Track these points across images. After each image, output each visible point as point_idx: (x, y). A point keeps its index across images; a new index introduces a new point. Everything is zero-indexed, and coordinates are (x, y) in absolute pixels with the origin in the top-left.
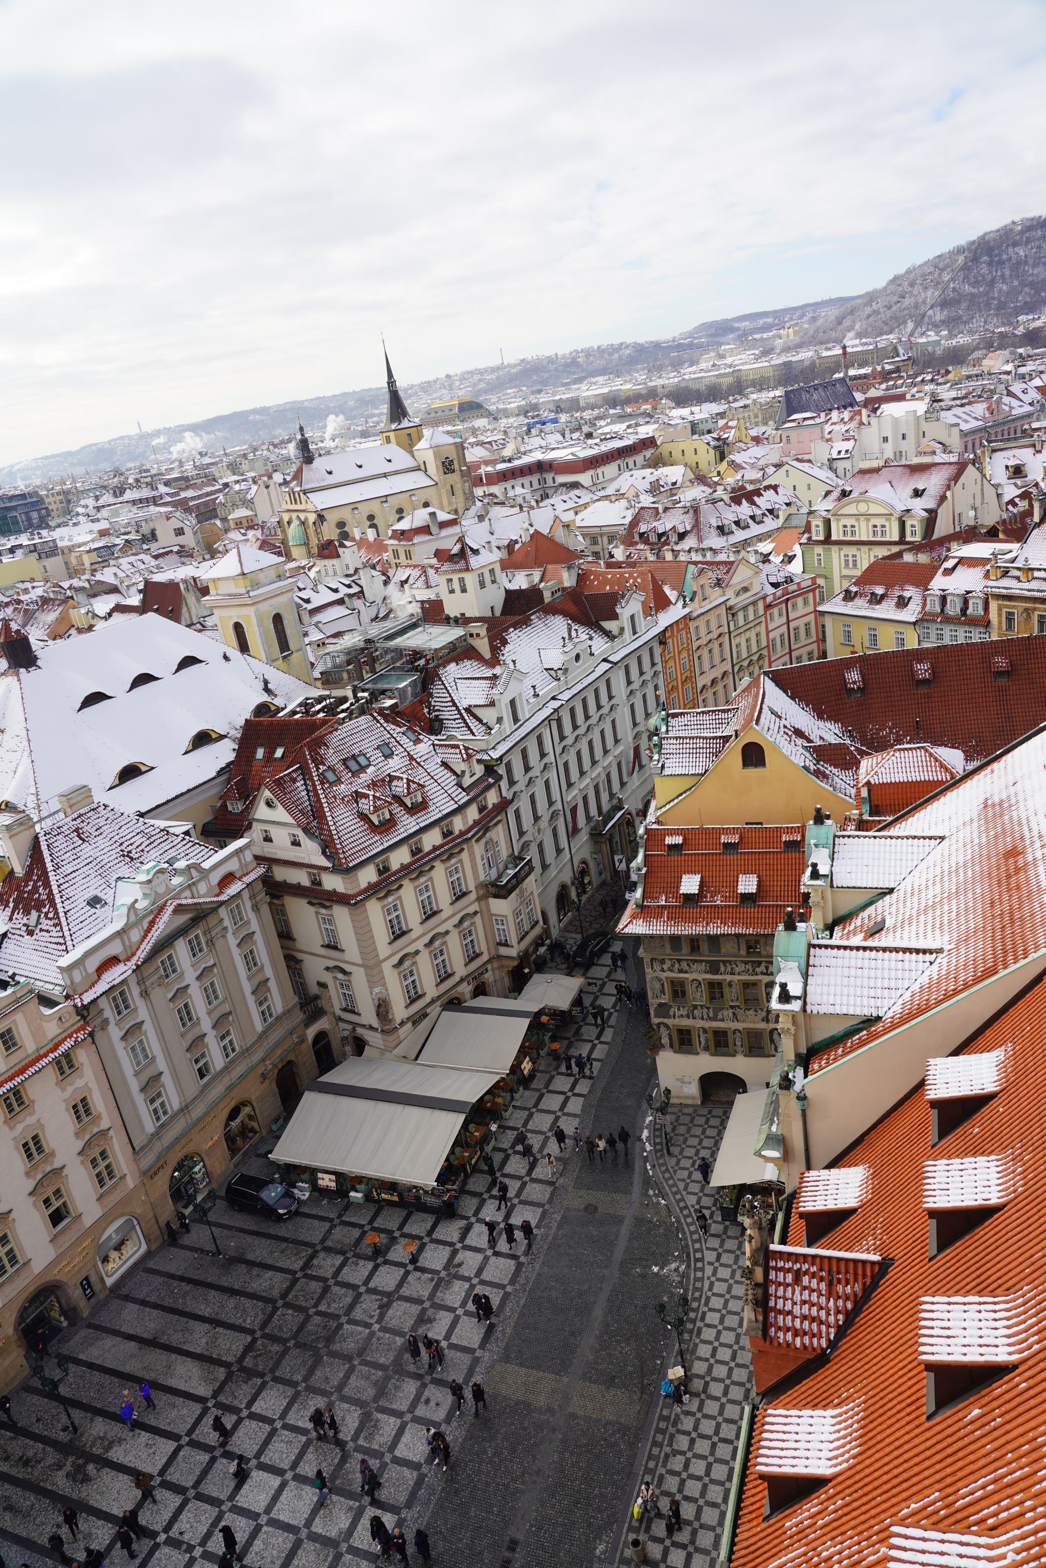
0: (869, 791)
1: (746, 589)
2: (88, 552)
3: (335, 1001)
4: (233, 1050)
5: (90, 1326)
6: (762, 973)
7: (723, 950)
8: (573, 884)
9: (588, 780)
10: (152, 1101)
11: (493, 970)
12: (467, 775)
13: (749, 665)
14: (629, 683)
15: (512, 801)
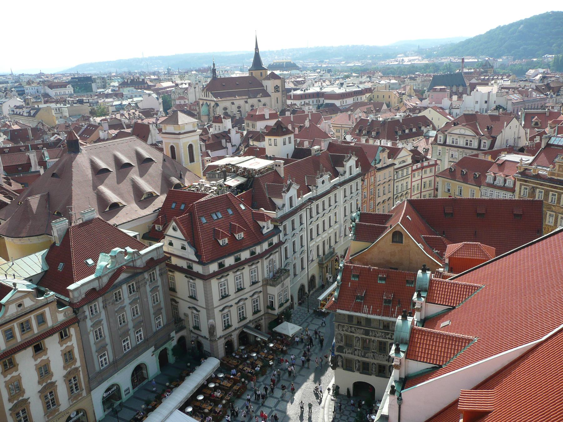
0: (449, 260)
1: (404, 162)
6: (389, 338)
7: (372, 325)
9: (320, 238)
11: (265, 319)
12: (266, 228)
13: (401, 196)
14: (345, 196)
15: (285, 243)
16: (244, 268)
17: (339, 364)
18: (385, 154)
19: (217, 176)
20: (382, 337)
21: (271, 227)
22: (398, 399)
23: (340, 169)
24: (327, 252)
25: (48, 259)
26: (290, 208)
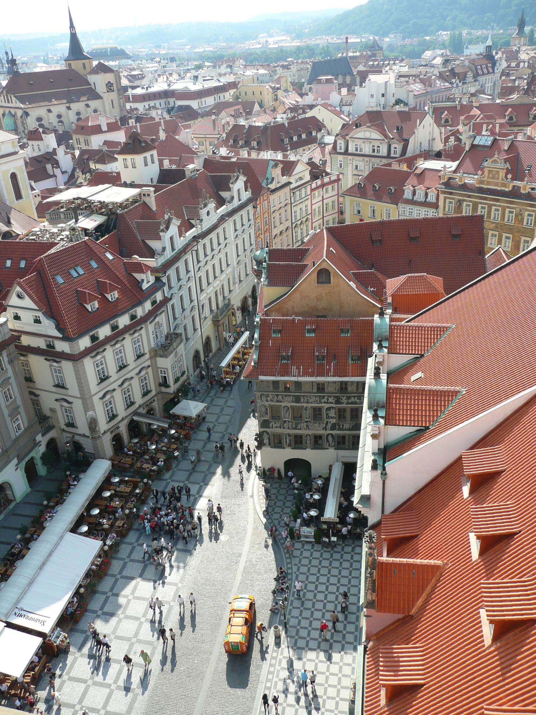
1: (301, 179)
6: (325, 403)
7: (303, 389)
9: (212, 288)
11: (158, 400)
12: (145, 282)
13: (301, 224)
14: (236, 230)
15: (171, 299)
16: (124, 338)
17: (265, 442)
18: (278, 171)
19: (62, 216)
20: (316, 402)
21: (152, 279)
22: (382, 474)
23: (225, 194)
24: (221, 305)
26: (173, 252)
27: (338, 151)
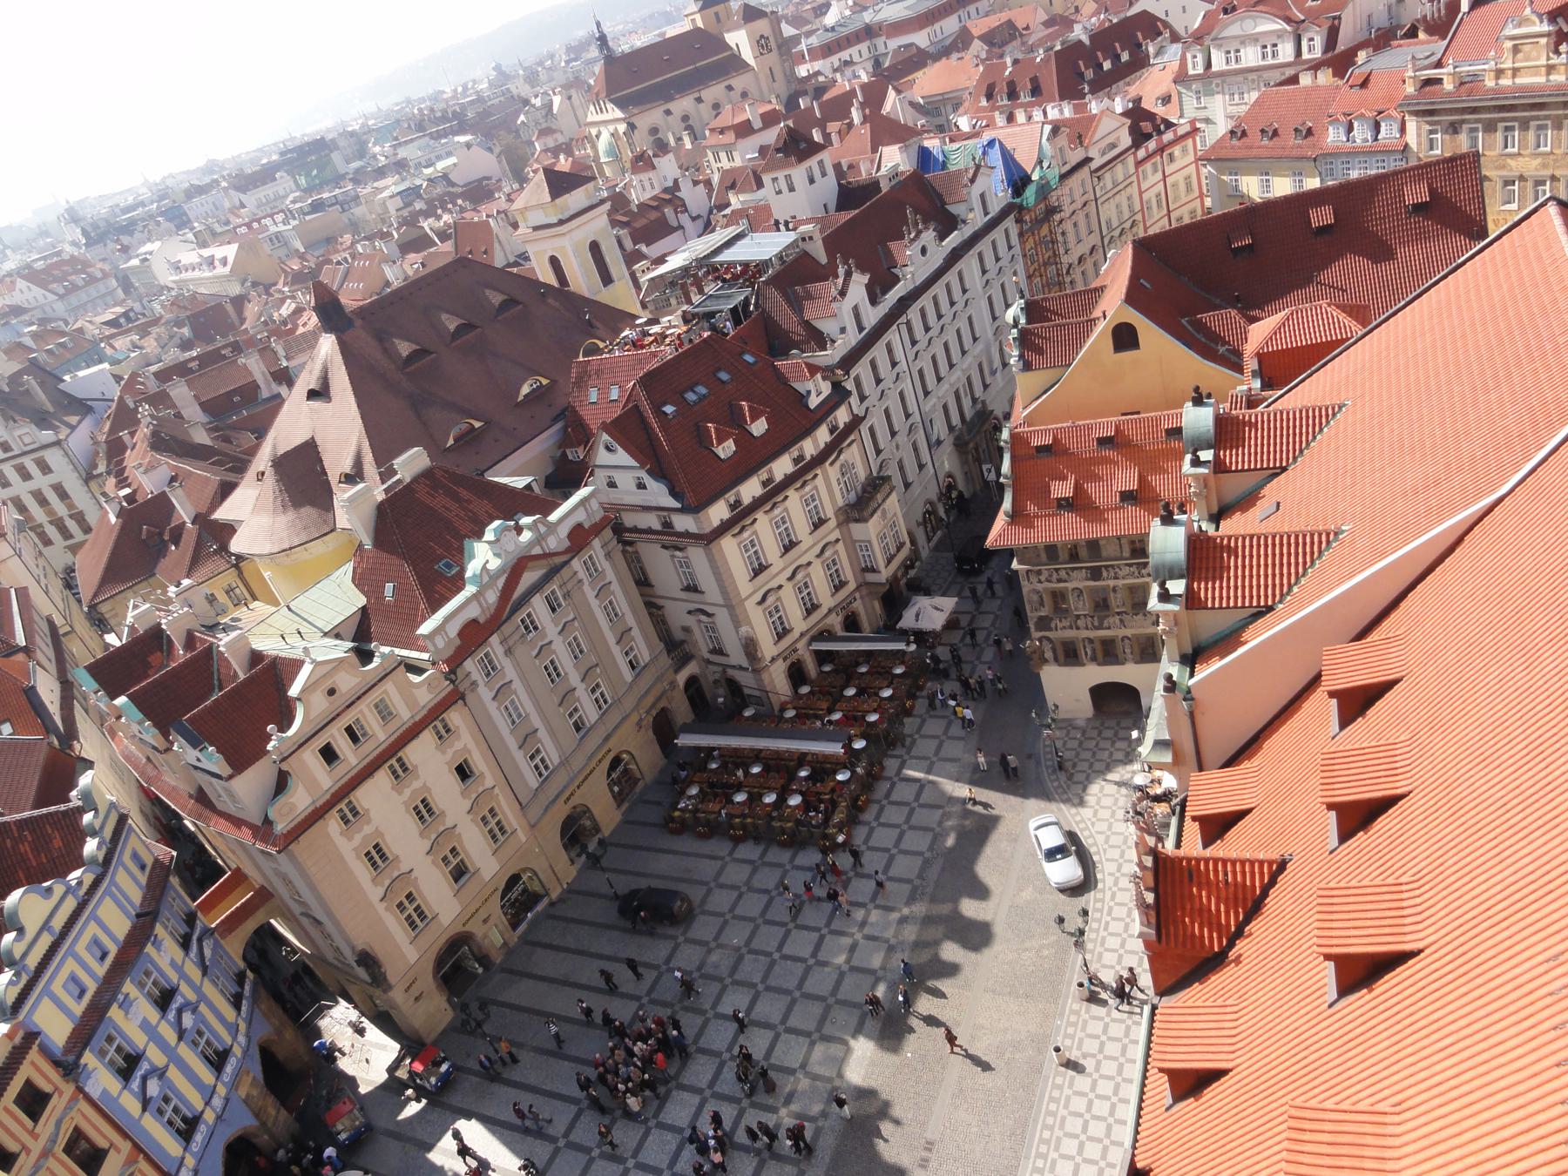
1: (1113, 146)
2: (391, 197)
3: (703, 646)
4: (605, 702)
5: (503, 970)
7: (1104, 554)
8: (940, 499)
10: (532, 757)
11: (862, 597)
12: (813, 394)
13: (1121, 234)
14: (984, 272)
15: (864, 418)
16: (786, 497)
17: (1046, 656)
20: (1132, 575)
21: (826, 388)
24: (969, 414)
25: (359, 581)
26: (860, 332)
27: (1191, 72)
